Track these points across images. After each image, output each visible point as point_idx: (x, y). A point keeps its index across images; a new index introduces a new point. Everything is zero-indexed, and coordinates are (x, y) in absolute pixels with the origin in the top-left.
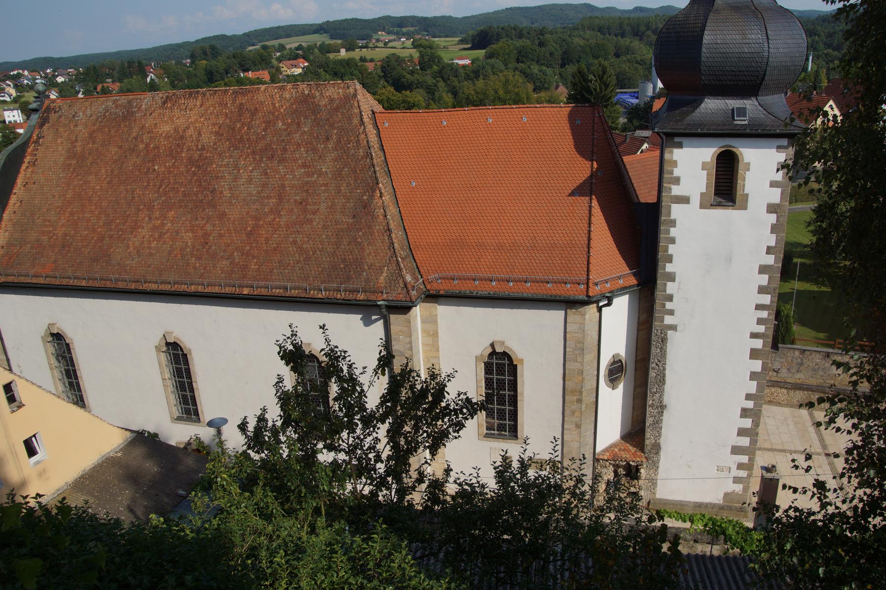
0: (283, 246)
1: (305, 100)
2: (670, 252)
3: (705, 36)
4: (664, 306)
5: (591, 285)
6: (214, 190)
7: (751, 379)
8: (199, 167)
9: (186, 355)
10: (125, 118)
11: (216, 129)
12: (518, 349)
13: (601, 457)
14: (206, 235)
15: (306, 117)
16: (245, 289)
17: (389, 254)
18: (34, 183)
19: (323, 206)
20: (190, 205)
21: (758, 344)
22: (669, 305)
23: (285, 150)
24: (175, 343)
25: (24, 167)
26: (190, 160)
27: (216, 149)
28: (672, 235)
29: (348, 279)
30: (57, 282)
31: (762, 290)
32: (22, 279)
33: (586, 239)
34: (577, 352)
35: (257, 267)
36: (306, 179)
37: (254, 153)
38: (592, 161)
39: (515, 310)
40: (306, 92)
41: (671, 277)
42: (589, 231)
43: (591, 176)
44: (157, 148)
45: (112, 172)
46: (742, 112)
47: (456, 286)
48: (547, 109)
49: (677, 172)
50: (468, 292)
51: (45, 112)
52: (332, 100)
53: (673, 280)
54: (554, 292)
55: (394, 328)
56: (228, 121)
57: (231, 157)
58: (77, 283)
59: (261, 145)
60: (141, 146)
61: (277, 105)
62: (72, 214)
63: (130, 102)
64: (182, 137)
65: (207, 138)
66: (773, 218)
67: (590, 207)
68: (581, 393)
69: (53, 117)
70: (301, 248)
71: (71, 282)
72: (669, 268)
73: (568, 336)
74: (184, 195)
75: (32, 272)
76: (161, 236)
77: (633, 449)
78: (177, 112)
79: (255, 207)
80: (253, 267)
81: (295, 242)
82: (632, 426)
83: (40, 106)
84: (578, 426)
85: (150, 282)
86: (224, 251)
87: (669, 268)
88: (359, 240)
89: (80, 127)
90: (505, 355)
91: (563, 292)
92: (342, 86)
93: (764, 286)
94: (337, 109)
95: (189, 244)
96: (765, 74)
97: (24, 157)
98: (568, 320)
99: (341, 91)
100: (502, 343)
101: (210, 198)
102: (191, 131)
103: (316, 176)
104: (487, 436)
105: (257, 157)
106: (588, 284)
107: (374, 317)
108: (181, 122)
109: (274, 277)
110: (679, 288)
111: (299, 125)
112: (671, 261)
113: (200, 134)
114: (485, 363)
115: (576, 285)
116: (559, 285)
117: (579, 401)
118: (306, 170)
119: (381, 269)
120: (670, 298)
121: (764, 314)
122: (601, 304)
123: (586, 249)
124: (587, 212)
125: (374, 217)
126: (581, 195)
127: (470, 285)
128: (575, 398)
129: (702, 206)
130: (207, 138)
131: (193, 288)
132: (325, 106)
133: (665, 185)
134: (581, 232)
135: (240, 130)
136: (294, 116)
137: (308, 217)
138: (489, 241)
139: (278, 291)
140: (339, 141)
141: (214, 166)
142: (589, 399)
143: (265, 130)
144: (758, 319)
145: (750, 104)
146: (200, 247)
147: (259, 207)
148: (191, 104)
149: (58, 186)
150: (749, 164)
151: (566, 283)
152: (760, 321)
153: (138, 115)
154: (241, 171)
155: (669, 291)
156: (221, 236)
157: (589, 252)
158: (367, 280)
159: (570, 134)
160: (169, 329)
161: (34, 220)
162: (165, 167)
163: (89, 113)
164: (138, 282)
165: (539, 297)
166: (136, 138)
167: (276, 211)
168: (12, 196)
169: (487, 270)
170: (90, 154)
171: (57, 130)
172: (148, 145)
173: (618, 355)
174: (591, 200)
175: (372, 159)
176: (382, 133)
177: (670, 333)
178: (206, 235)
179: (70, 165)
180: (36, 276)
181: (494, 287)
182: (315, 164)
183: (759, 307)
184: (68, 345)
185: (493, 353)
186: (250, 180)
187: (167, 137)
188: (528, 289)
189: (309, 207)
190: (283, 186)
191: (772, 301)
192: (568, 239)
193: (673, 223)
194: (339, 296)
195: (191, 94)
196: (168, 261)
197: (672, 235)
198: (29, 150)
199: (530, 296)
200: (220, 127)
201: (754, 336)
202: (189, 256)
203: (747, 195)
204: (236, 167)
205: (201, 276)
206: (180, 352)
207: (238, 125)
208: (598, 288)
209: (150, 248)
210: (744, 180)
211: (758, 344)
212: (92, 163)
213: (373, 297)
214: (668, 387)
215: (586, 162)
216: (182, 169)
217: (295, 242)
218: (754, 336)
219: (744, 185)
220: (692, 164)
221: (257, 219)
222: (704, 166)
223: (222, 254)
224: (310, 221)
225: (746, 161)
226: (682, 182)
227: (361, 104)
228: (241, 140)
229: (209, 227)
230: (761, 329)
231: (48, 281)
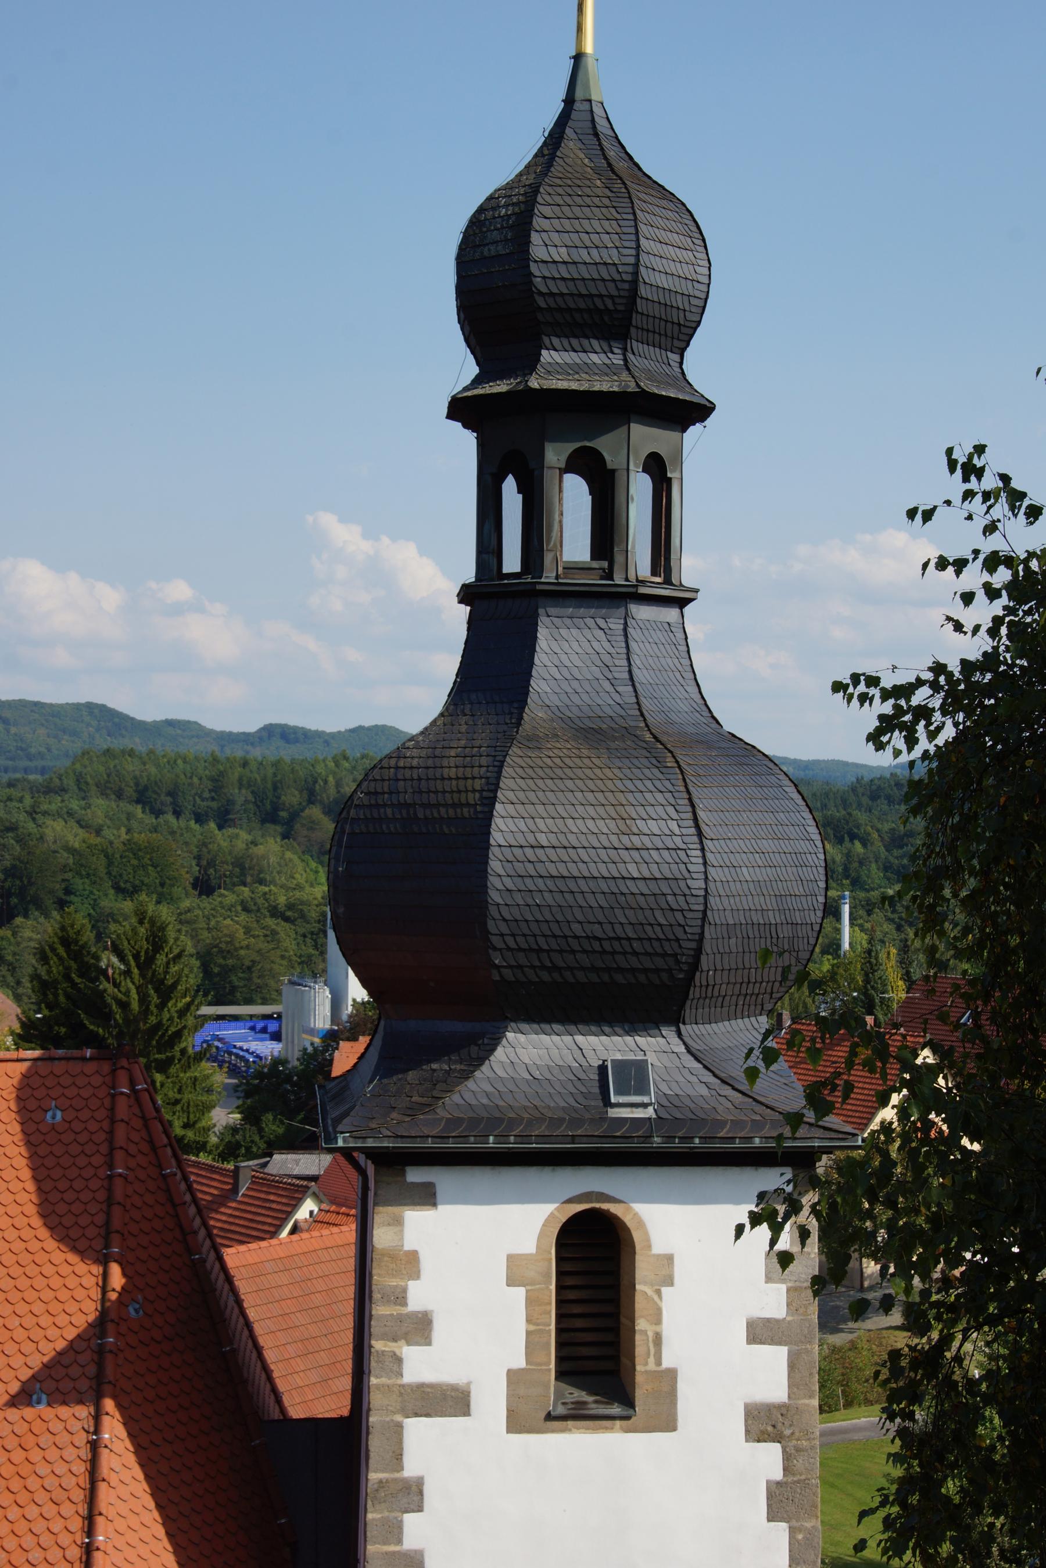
3: (498, 822)
38: (104, 1261)
49: (419, 1296)
66: (768, 1460)
67: (94, 1446)
96: (699, 951)
124: (80, 1468)
126: (60, 1397)
129: (516, 1423)
133: (378, 1345)
145: (656, 1050)
150: (669, 1259)
159: (21, 1163)
174: (97, 1418)
193: (412, 1494)
210: (658, 1320)
215: (82, 1268)
219: (658, 1340)
220: (472, 1264)
222: (516, 1272)
225: (659, 1247)
226: (439, 1330)
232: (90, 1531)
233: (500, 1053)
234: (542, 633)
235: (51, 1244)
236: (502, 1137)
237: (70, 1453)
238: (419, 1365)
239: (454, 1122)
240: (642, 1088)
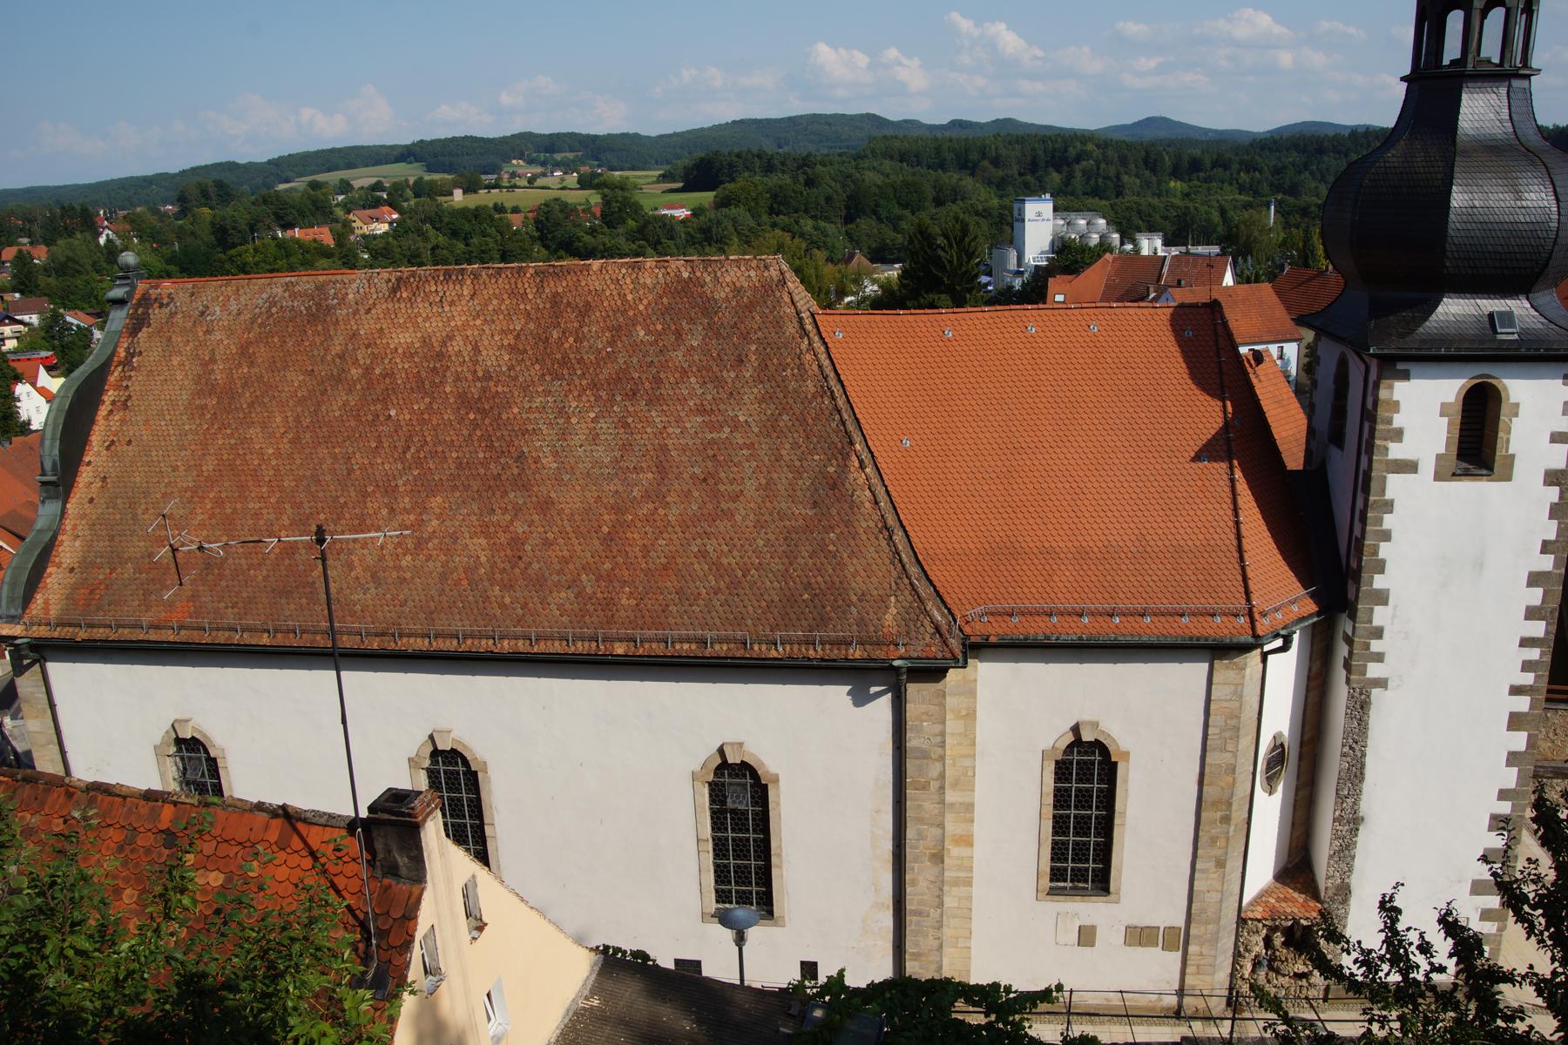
0: (679, 561)
1: (684, 289)
2: (1381, 555)
4: (1367, 646)
5: (1257, 616)
6: (521, 458)
7: (1509, 763)
8: (484, 413)
10: (313, 318)
12: (1119, 734)
13: (1250, 915)
14: (516, 542)
15: (691, 321)
16: (617, 645)
17: (894, 574)
18: (129, 443)
19: (750, 487)
20: (475, 485)
21: (1523, 704)
22: (1376, 646)
23: (657, 381)
25: (103, 411)
26: (464, 400)
27: (516, 378)
28: (1385, 526)
29: (823, 621)
30: (206, 638)
31: (1531, 614)
32: (126, 634)
33: (1232, 537)
34: (1227, 734)
36: (709, 436)
37: (594, 386)
39: (1120, 666)
40: (686, 275)
41: (1382, 598)
42: (1237, 523)
43: (1227, 426)
45: (298, 420)
46: (1508, 318)
47: (1017, 627)
48: (1131, 311)
49: (1398, 421)
50: (1041, 637)
51: (139, 304)
52: (738, 290)
53: (1385, 603)
54: (1195, 632)
55: (912, 709)
56: (532, 326)
57: (547, 393)
58: (248, 639)
59: (605, 373)
61: (630, 297)
62: (219, 502)
63: (320, 288)
64: (440, 356)
65: (493, 357)
66: (1553, 494)
67: (1232, 481)
68: (1230, 805)
69: (156, 314)
70: (717, 566)
71: (236, 638)
72: (1379, 582)
73: (1213, 706)
74: (460, 466)
75: (146, 620)
76: (420, 544)
77: (1300, 898)
78: (422, 307)
79: (613, 488)
80: (624, 601)
82: (1289, 855)
83: (130, 294)
84: (1221, 864)
85: (409, 636)
86: (560, 572)
87: (1379, 582)
88: (831, 548)
89: (218, 335)
90: (1099, 746)
91: (1211, 632)
92: (754, 264)
93: (1536, 607)
94: (751, 307)
95: (483, 559)
98: (1215, 680)
99: (752, 273)
100: (1095, 725)
101: (516, 471)
102: (457, 344)
103: (727, 430)
104: (1053, 892)
105: (603, 394)
106: (1250, 614)
107: (874, 690)
108: (434, 327)
110: (1394, 616)
111: (679, 335)
112: (1382, 571)
113: (476, 350)
114: (1057, 762)
115: (1232, 619)
116: (1201, 619)
117: (1226, 819)
118: (707, 418)
119: (883, 600)
120: (1378, 633)
121: (1534, 654)
122: (1266, 648)
123: (1236, 555)
124: (1227, 489)
125: (854, 506)
126: (1212, 459)
127: (1042, 625)
128: (1219, 814)
129: (1438, 477)
130: (493, 357)
131: (506, 646)
132: (727, 300)
133: (1378, 442)
134: (1222, 524)
135: (560, 342)
137: (724, 505)
138: (1062, 544)
139: (686, 646)
140: (763, 366)
141: (516, 410)
142: (1238, 814)
143: (612, 343)
144: (1524, 663)
145: (1519, 307)
146: (507, 566)
149: (182, 448)
151: (1213, 615)
152: (1527, 666)
153: (342, 313)
154: (574, 420)
155: (1376, 622)
156: (547, 543)
157: (1242, 559)
158: (861, 622)
159: (1178, 354)
160: (442, 725)
161: (135, 516)
162: (412, 412)
163: (234, 307)
164: (383, 634)
165: (1169, 641)
166: (341, 356)
167: (656, 496)
168: (82, 469)
169: (1068, 596)
170: (245, 385)
171: (169, 339)
172: (368, 370)
173: (1280, 734)
174: (1231, 468)
175: (833, 398)
176: (833, 350)
177: (1375, 692)
178: (516, 542)
180: (157, 627)
181: (1085, 627)
182: (722, 407)
183: (1526, 642)
184: (213, 764)
185: (1077, 743)
186: (594, 438)
187: (409, 355)
188: (1148, 629)
189: (722, 488)
190: (664, 449)
191: (1547, 632)
192: (1201, 537)
193: (1389, 506)
194: (811, 653)
195: (448, 275)
196: (442, 592)
197: (1385, 526)
198: (112, 379)
199: (1154, 640)
200: (517, 337)
201: (1516, 690)
202: (486, 584)
203: (1513, 456)
204: (561, 411)
206: (461, 769)
207: (555, 335)
208: (1266, 621)
209: (398, 568)
211: (1523, 704)
212: (251, 405)
213: (879, 654)
214: (1367, 786)
216: (448, 415)
217: (703, 554)
218: (1516, 690)
220: (1421, 408)
221: (618, 510)
222: (1444, 410)
223: (555, 578)
224: (729, 515)
226: (1406, 437)
227: (796, 298)
228: (565, 362)
229: (520, 528)
230: (1528, 679)
231: (184, 636)
232: (1236, 515)
233: (1440, 309)
234: (1464, 96)
235: (1198, 392)
236: (1448, 349)
237: (1222, 483)
238: (1396, 451)
239: (1423, 341)
240: (1512, 325)
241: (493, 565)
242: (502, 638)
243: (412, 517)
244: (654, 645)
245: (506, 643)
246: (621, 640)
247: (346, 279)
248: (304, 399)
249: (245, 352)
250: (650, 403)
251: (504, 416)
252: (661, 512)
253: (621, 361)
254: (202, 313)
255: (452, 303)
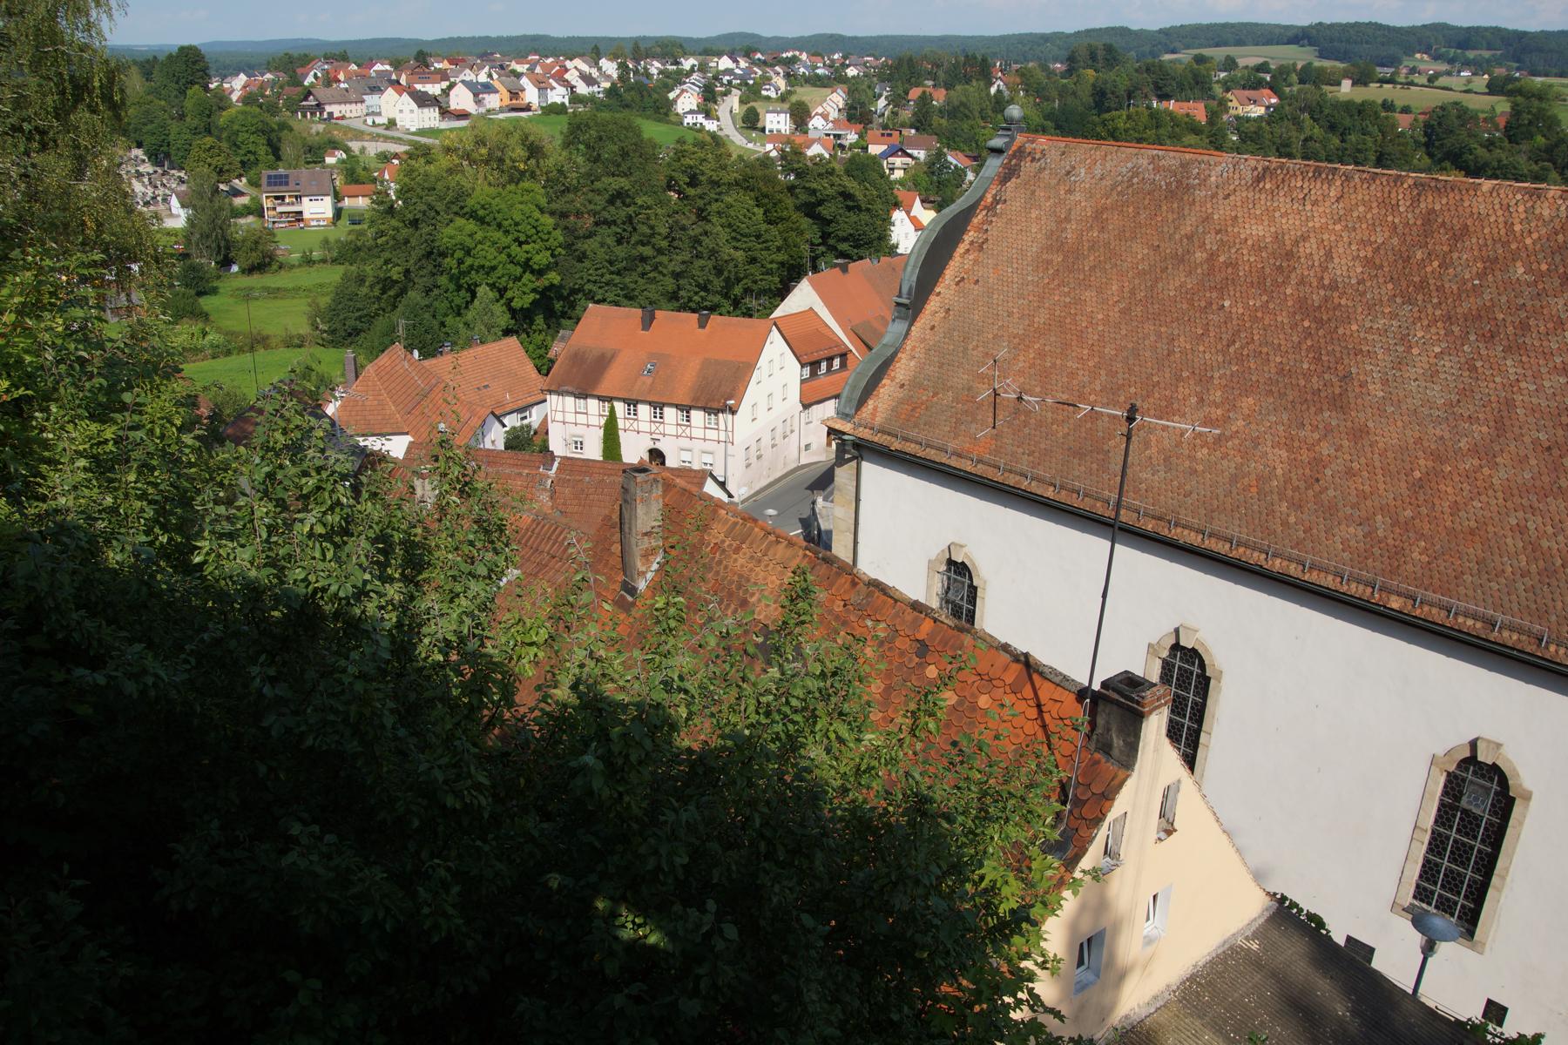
0: (1491, 529)
6: (1347, 377)
8: (1320, 323)
9: (1208, 679)
10: (1171, 194)
11: (1368, 252)
14: (1318, 463)
16: (1393, 597)
18: (977, 282)
23: (1524, 327)
24: (1194, 650)
25: (961, 249)
26: (1303, 306)
27: (1363, 294)
35: (1425, 558)
37: (1449, 319)
44: (1233, 264)
45: (1133, 292)
51: (1014, 156)
56: (1395, 241)
58: (1035, 488)
60: (1200, 256)
61: (1517, 228)
62: (1041, 355)
64: (1289, 255)
65: (1345, 266)
69: (1027, 167)
70: (1535, 547)
71: (1025, 484)
74: (1280, 372)
75: (951, 446)
78: (1282, 202)
79: (1438, 432)
80: (1415, 555)
81: (1521, 529)
86: (1355, 506)
89: (1077, 196)
95: (1279, 472)
97: (964, 231)
101: (1337, 391)
102: (1310, 246)
105: (1456, 329)
108: (1291, 225)
109: (1462, 590)
113: (1329, 255)
130: (1345, 266)
131: (1277, 565)
135: (1422, 264)
136: (1558, 258)
139: (1470, 622)
141: (1355, 327)
143: (1481, 275)
146: (1302, 485)
147: (1447, 436)
148: (1316, 193)
153: (1200, 194)
154: (1415, 351)
160: (1190, 622)
163: (1098, 171)
164: (1160, 519)
166: (1189, 237)
167: (1485, 453)
168: (932, 297)
170: (1091, 248)
171: (1033, 192)
178: (1318, 463)
179: (1049, 262)
180: (960, 456)
184: (973, 590)
186: (1433, 374)
187: (1258, 248)
190: (1510, 404)
198: (975, 221)
202: (1276, 497)
205: (1298, 544)
206: (1196, 670)
207: (1419, 255)
209: (1191, 458)
212: (1093, 268)
216: (1283, 318)
217: (1521, 529)
221: (1437, 457)
223: (1348, 511)
228: (1422, 286)
229: (1326, 449)
231: (980, 469)
241: (1288, 481)
242: (1275, 556)
243: (1219, 412)
244: (1434, 610)
245: (1278, 561)
246: (1399, 594)
247: (1212, 160)
248: (1144, 272)
249: (1098, 214)
250: (1508, 350)
251: (1341, 331)
252: (1486, 471)
253: (1487, 297)
254: (1068, 173)
255: (1315, 203)
